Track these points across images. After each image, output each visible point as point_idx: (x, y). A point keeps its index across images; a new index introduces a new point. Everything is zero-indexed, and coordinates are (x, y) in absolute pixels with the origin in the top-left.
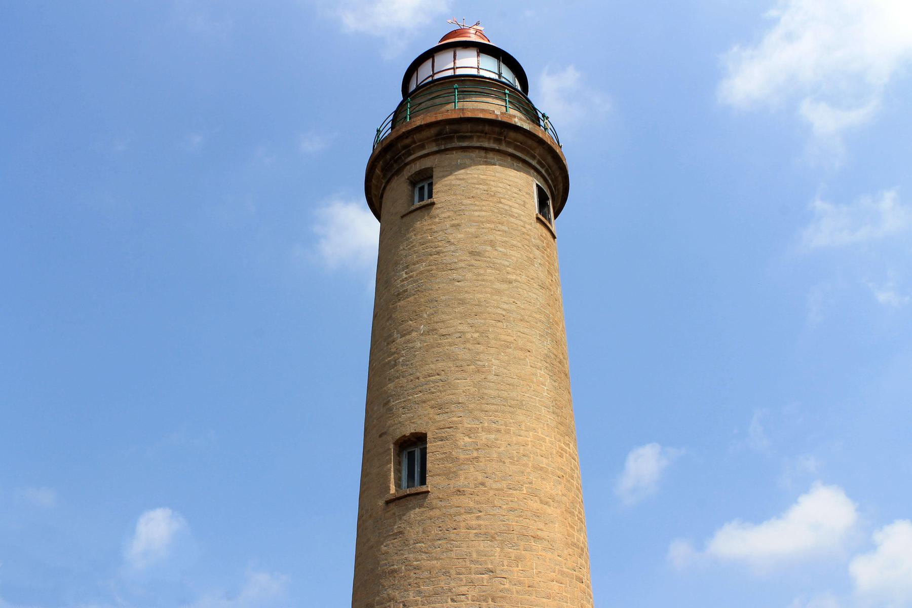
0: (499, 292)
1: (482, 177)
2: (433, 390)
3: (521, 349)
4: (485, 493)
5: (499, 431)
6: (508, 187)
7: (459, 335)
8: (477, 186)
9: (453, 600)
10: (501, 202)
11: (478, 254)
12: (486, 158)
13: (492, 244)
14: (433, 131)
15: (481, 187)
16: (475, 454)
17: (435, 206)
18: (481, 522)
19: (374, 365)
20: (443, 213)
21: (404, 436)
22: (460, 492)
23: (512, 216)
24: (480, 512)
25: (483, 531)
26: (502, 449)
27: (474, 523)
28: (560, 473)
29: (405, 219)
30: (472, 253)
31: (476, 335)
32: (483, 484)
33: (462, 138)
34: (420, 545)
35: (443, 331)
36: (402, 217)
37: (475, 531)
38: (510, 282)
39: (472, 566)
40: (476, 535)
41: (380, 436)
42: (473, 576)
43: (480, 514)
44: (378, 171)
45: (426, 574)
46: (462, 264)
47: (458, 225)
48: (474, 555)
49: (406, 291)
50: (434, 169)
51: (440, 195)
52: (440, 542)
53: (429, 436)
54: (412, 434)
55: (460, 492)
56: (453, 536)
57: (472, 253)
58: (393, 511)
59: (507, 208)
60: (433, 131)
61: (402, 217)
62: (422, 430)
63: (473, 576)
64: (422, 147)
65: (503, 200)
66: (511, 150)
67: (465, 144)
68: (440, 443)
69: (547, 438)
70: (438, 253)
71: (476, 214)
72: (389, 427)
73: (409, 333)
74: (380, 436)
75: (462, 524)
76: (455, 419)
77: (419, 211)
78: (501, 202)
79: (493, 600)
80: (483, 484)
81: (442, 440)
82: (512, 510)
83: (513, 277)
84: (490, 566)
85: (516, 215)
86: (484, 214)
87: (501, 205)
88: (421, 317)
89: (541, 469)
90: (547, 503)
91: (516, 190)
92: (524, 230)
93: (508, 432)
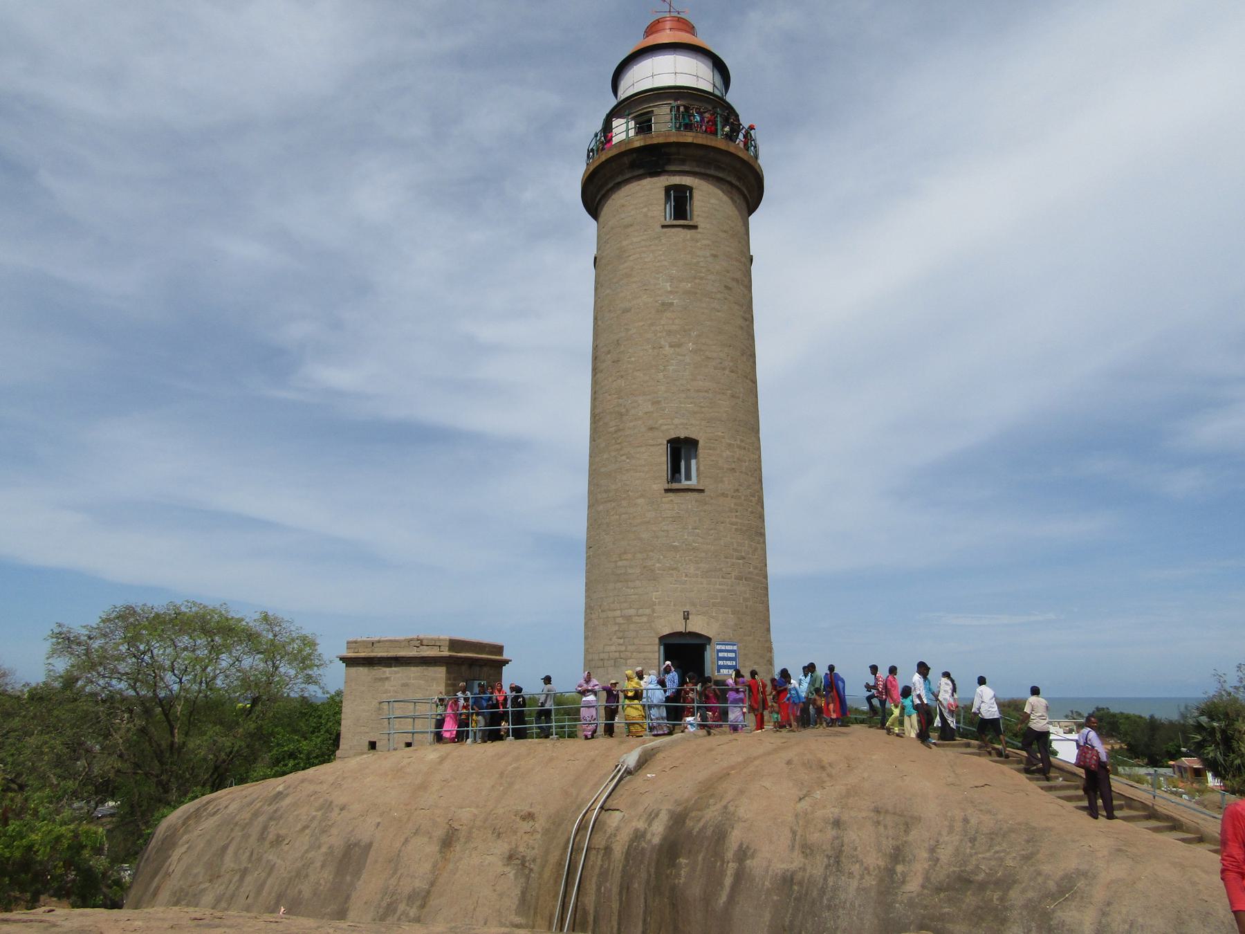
2: (702, 404)
4: (740, 497)
7: (720, 361)
9: (723, 577)
16: (733, 466)
19: (633, 359)
20: (704, 239)
21: (679, 438)
22: (724, 495)
24: (737, 512)
32: (738, 490)
33: (718, 168)
34: (698, 531)
35: (707, 353)
36: (663, 227)
37: (735, 527)
39: (735, 554)
40: (736, 530)
41: (651, 429)
42: (734, 561)
43: (737, 514)
44: (626, 160)
45: (703, 555)
46: (719, 296)
49: (672, 304)
50: (694, 190)
51: (700, 219)
52: (712, 531)
53: (701, 444)
54: (686, 437)
55: (724, 495)
56: (722, 529)
58: (671, 498)
61: (663, 227)
62: (693, 436)
63: (734, 561)
64: (683, 162)
67: (721, 175)
68: (711, 451)
70: (701, 278)
72: (661, 425)
73: (679, 345)
74: (651, 429)
76: (720, 434)
80: (738, 490)
81: (710, 449)
84: (743, 554)
88: (690, 334)
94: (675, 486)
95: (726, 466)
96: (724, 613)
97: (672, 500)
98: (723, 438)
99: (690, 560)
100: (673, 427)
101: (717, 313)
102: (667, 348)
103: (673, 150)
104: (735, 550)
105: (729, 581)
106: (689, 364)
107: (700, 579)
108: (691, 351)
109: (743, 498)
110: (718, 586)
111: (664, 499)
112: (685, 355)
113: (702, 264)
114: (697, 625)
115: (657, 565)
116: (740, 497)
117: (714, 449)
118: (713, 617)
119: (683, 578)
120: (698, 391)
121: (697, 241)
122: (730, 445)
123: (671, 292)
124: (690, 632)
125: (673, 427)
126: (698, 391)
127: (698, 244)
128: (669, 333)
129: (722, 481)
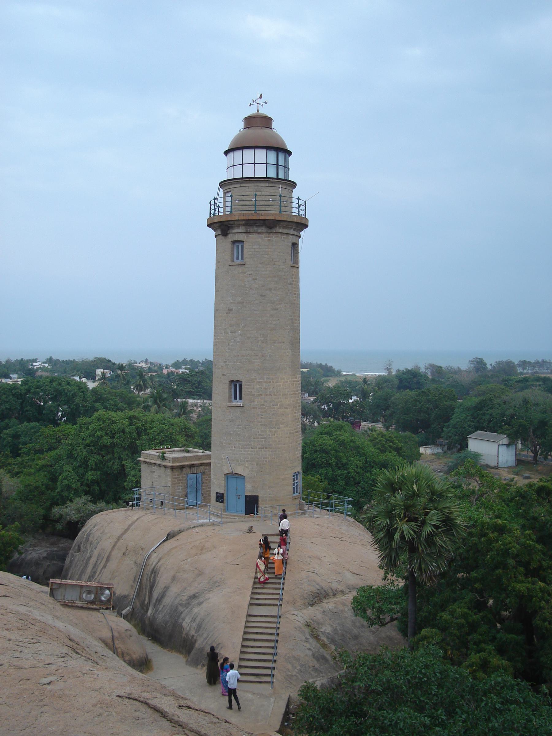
0: (272, 316)
1: (267, 250)
3: (280, 343)
5: (270, 382)
6: (279, 254)
7: (255, 338)
8: (264, 256)
9: (252, 448)
10: (275, 264)
11: (264, 296)
12: (269, 237)
13: (270, 289)
14: (244, 222)
15: (266, 256)
16: (261, 393)
17: (246, 266)
18: (262, 420)
22: (254, 408)
23: (280, 271)
25: (263, 423)
26: (271, 390)
27: (260, 420)
28: (292, 393)
29: (231, 267)
30: (261, 296)
31: (262, 339)
32: (264, 405)
38: (277, 309)
40: (261, 425)
42: (259, 440)
47: (256, 279)
48: (260, 432)
49: (232, 310)
55: (254, 408)
57: (261, 296)
59: (278, 267)
60: (244, 222)
65: (276, 263)
66: (281, 231)
68: (247, 387)
69: (288, 380)
71: (264, 273)
73: (234, 332)
74: (223, 375)
75: (256, 420)
76: (253, 377)
77: (237, 266)
78: (275, 264)
79: (266, 448)
80: (264, 405)
82: (274, 414)
83: (278, 307)
84: (265, 436)
85: (282, 270)
86: (267, 272)
87: (275, 266)
89: (285, 394)
90: (287, 408)
91: (282, 254)
92: (285, 277)
93: (273, 382)
94: (235, 403)
95: (256, 393)
96: (253, 465)
97: (230, 411)
98: (256, 379)
99: (237, 440)
100: (231, 375)
101: (255, 312)
102: (230, 333)
103: (231, 223)
104: (259, 435)
105: (255, 450)
106: (239, 342)
107: (240, 449)
108: (240, 335)
109: (267, 408)
110: (249, 453)
111: (227, 410)
112: (237, 337)
113: (247, 286)
114: (239, 470)
115: (224, 441)
116: (265, 408)
117: (250, 385)
118: (246, 467)
119: (234, 449)
120: (243, 356)
121: (245, 273)
122: (259, 382)
123: (232, 303)
124: (236, 473)
125: (231, 375)
126: (243, 356)
127: (246, 274)
128: (231, 325)
129: (254, 401)
